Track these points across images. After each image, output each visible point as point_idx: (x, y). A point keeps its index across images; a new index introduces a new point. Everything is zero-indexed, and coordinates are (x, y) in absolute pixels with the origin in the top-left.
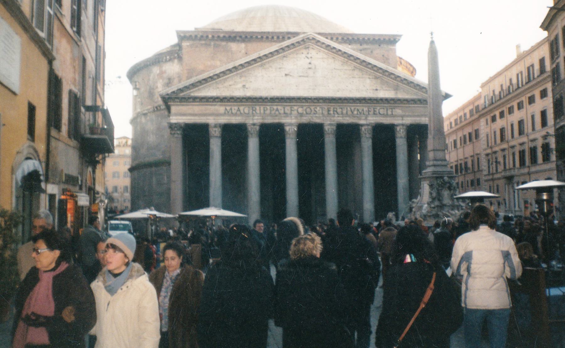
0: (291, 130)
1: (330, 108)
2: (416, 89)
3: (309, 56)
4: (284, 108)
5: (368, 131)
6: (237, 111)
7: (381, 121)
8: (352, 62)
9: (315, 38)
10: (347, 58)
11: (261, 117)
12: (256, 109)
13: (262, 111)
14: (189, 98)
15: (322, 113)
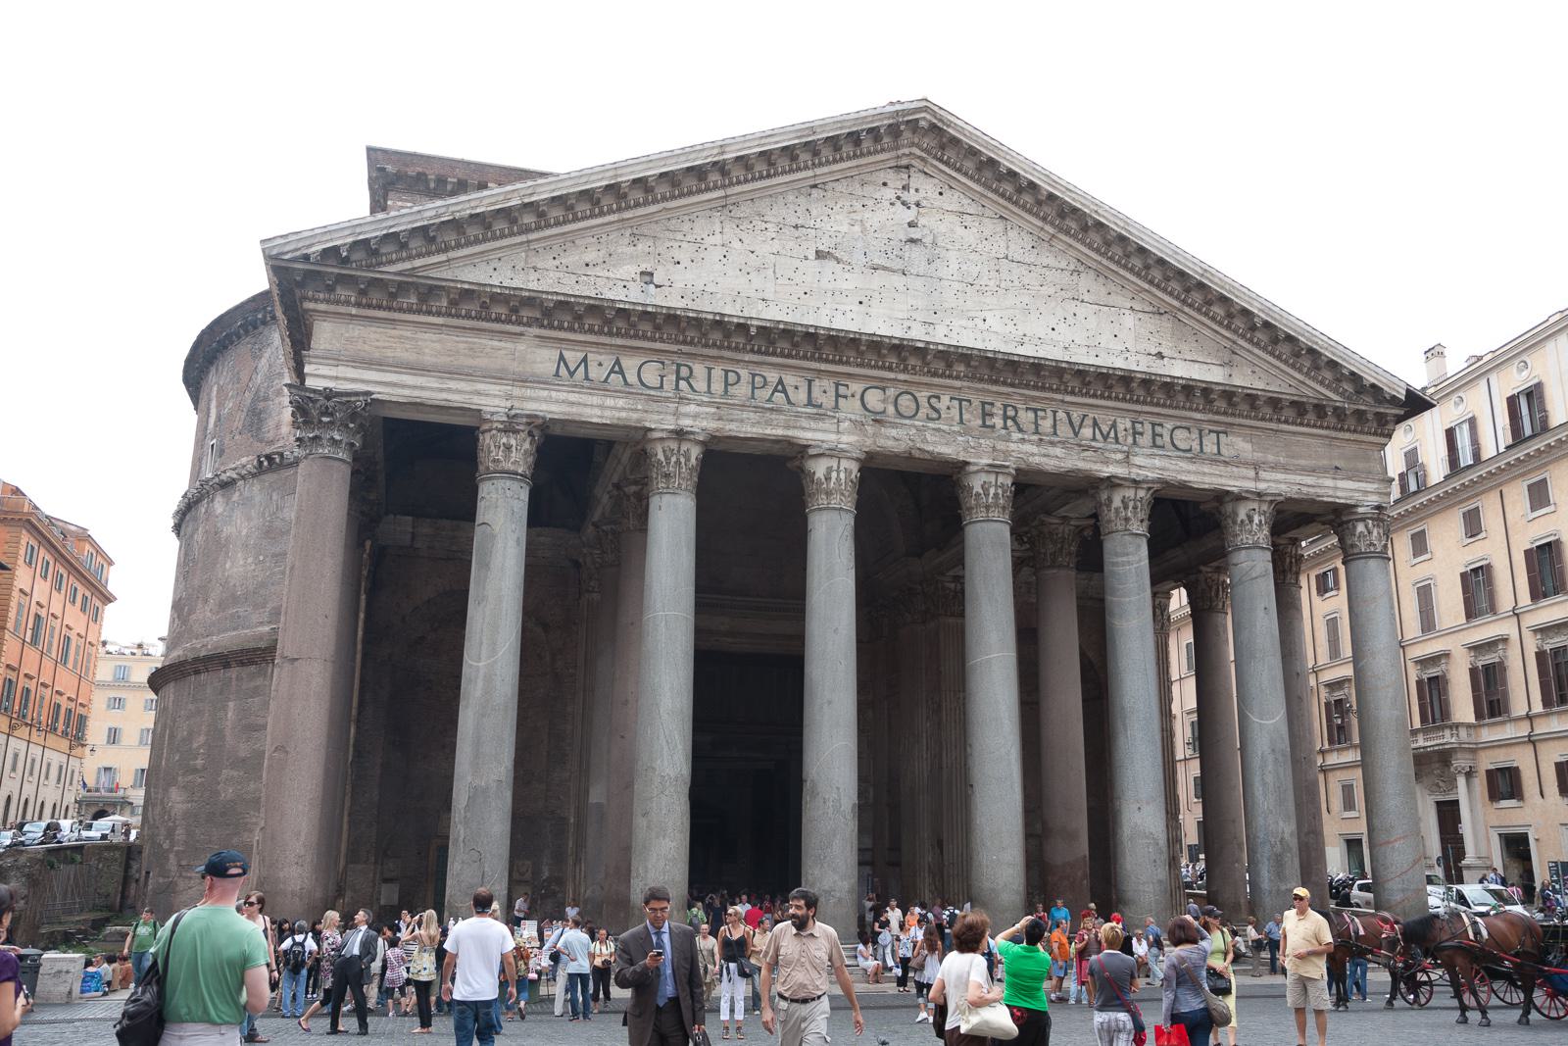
0: (834, 475)
1: (992, 404)
2: (1300, 371)
3: (911, 197)
4: (810, 382)
5: (1135, 508)
6: (612, 371)
7: (1184, 478)
8: (1070, 241)
9: (940, 124)
10: (1052, 224)
11: (713, 410)
12: (690, 368)
13: (718, 387)
14: (403, 288)
15: (961, 421)
